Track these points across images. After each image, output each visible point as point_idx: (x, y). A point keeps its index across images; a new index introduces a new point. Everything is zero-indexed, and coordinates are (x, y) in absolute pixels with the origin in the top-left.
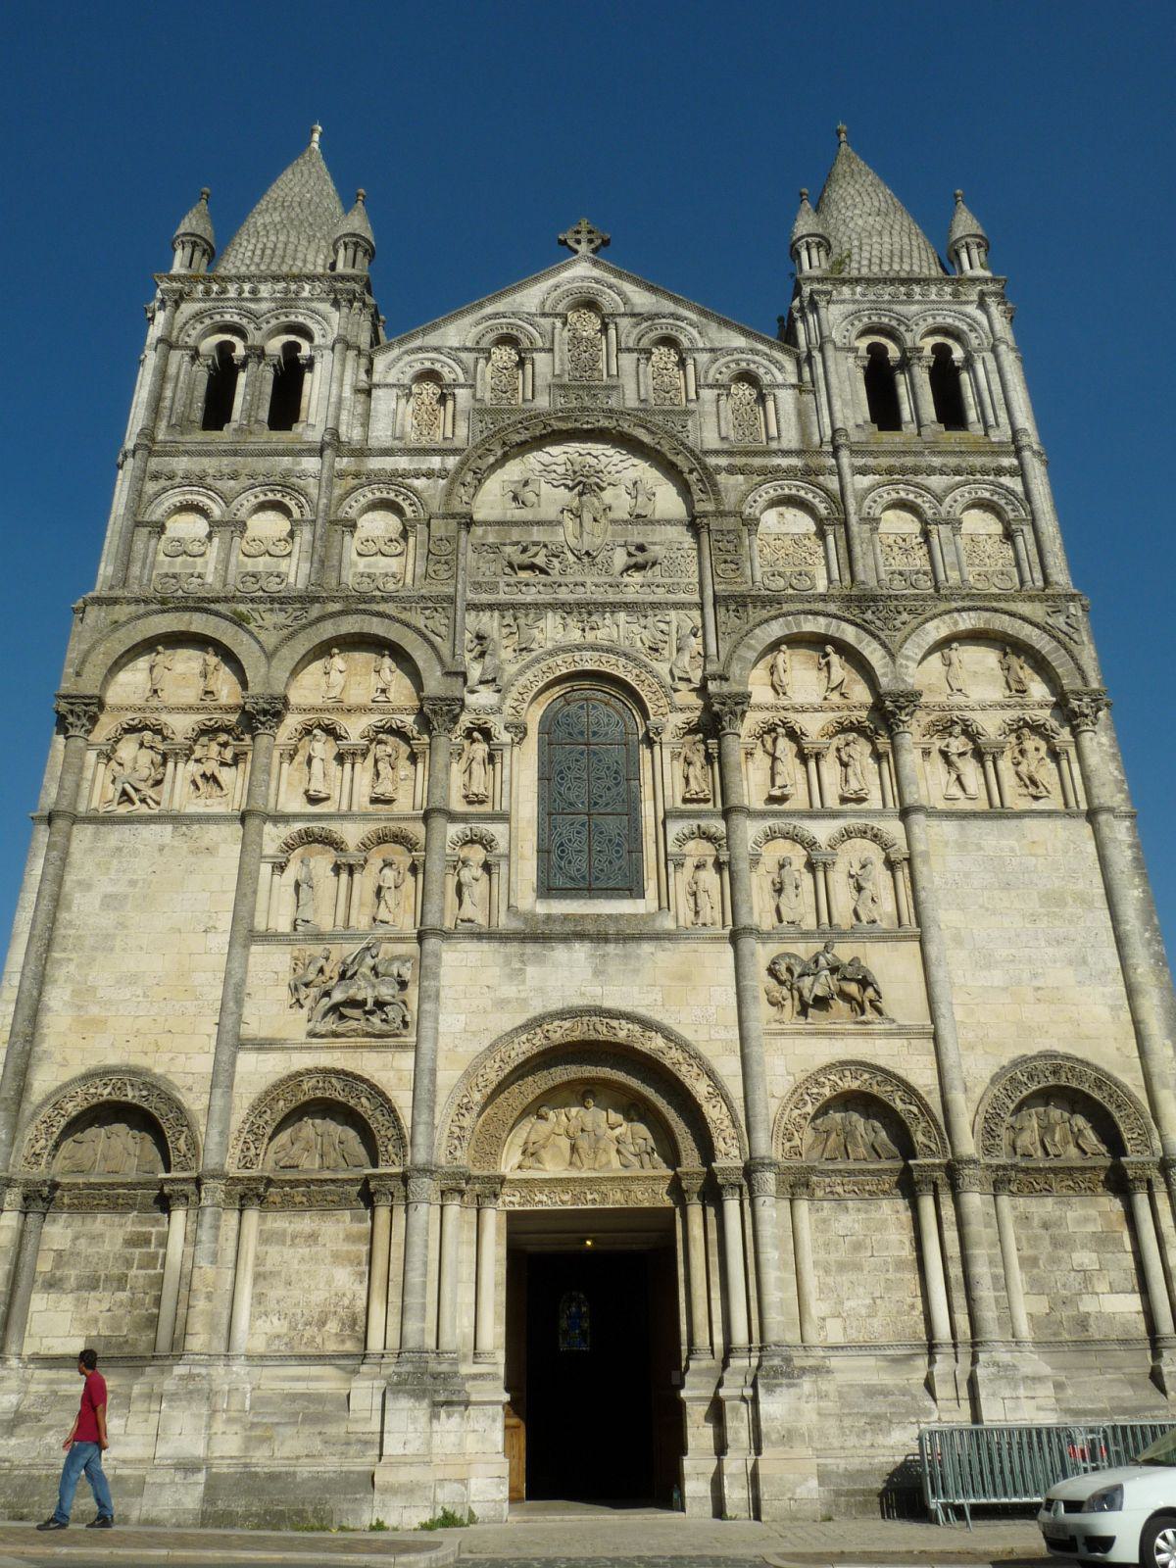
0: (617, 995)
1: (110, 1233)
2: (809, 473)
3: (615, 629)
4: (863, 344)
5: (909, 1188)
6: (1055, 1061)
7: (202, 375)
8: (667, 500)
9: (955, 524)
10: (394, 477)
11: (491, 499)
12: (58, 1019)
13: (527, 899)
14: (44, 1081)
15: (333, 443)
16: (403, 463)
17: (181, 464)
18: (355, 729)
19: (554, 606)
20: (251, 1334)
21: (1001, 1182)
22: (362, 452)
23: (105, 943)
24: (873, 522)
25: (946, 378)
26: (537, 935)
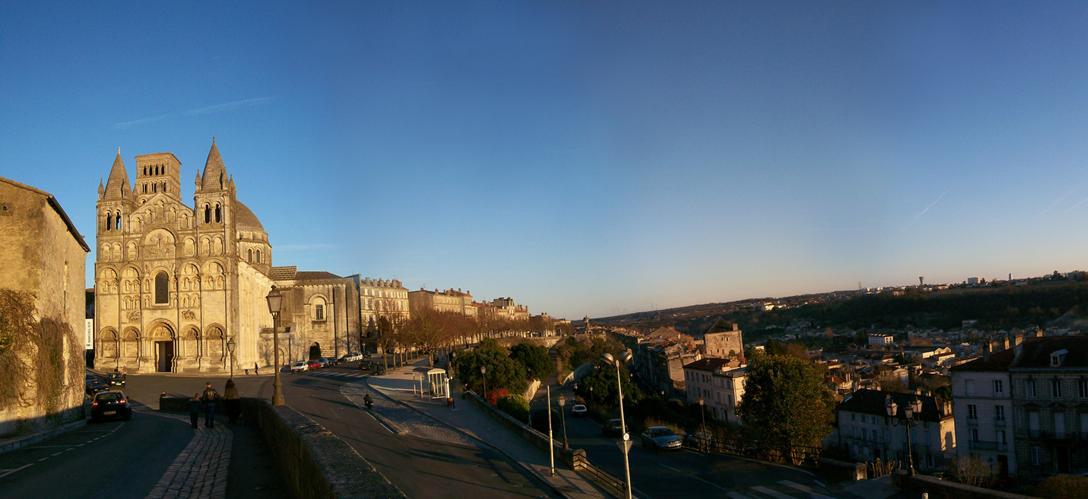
0: (165, 317)
1: (111, 344)
2: (193, 234)
3: (165, 263)
4: (204, 206)
5: (197, 339)
6: (216, 324)
7: (106, 218)
8: (172, 240)
9: (213, 242)
10: (133, 238)
11: (147, 241)
12: (102, 321)
13: (154, 303)
14: (101, 328)
15: (124, 233)
16: (134, 236)
17: (105, 238)
18: (131, 280)
19: (156, 260)
20: (127, 355)
21: (207, 339)
22: (129, 234)
23: (105, 311)
24: (201, 242)
25: (218, 211)
26: (155, 309)
